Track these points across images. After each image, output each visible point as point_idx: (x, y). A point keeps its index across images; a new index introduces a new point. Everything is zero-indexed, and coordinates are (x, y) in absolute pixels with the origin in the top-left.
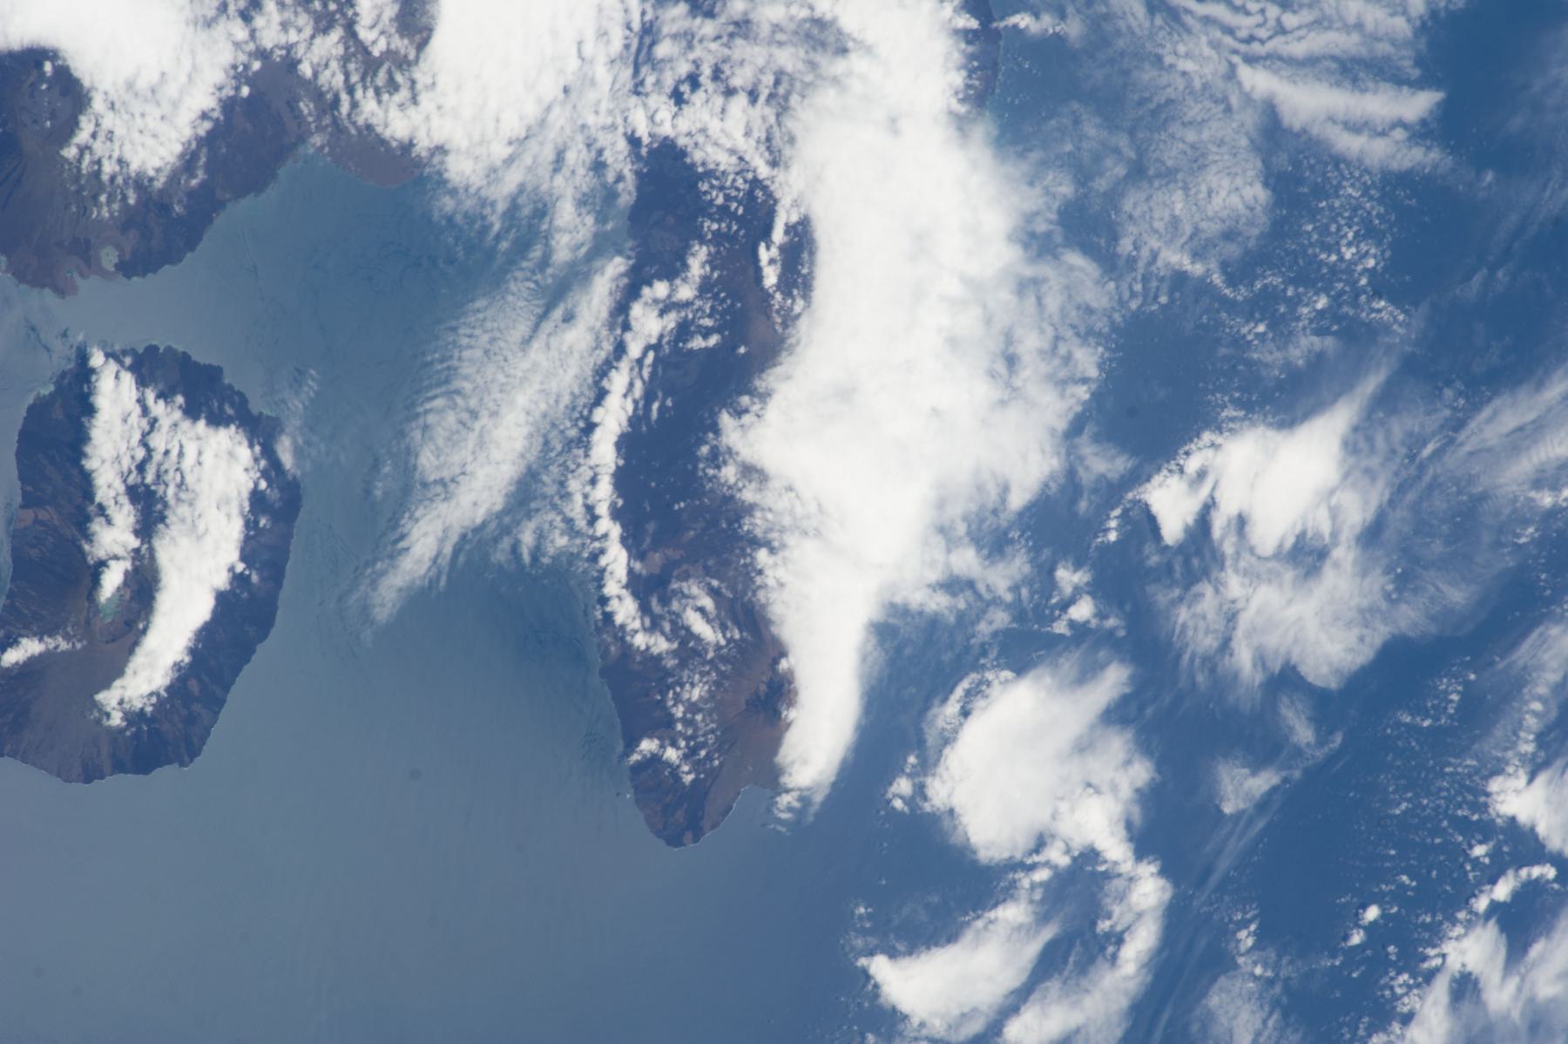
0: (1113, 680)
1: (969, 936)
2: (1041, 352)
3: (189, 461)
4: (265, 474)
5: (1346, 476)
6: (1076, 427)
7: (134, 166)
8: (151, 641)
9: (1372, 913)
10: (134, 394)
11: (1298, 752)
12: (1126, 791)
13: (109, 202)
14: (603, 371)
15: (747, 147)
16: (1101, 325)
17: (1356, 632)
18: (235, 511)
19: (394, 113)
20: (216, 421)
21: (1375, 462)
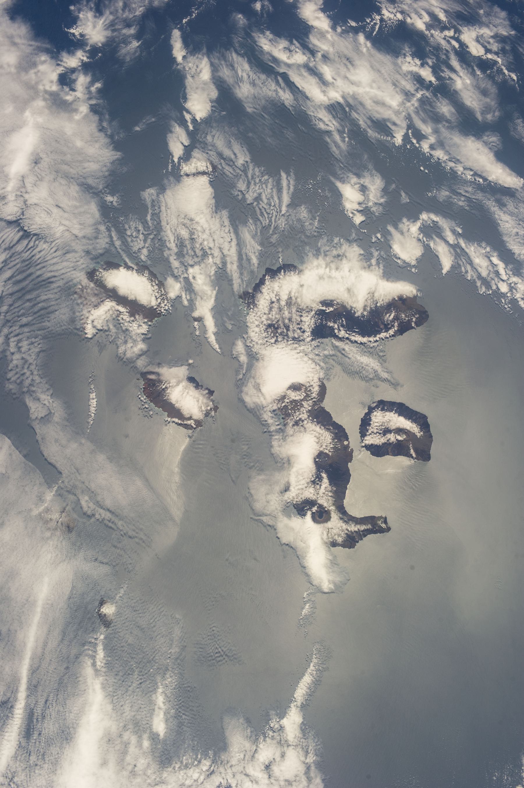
0: (390, 228)
1: (437, 253)
2: (336, 250)
3: (378, 424)
4: (378, 409)
5: (349, 182)
6: (348, 240)
7: (331, 441)
8: (408, 428)
10: (368, 437)
13: (337, 445)
14: (352, 342)
15: (310, 316)
16: (329, 237)
18: (384, 414)
19: (315, 390)
21: (345, 176)
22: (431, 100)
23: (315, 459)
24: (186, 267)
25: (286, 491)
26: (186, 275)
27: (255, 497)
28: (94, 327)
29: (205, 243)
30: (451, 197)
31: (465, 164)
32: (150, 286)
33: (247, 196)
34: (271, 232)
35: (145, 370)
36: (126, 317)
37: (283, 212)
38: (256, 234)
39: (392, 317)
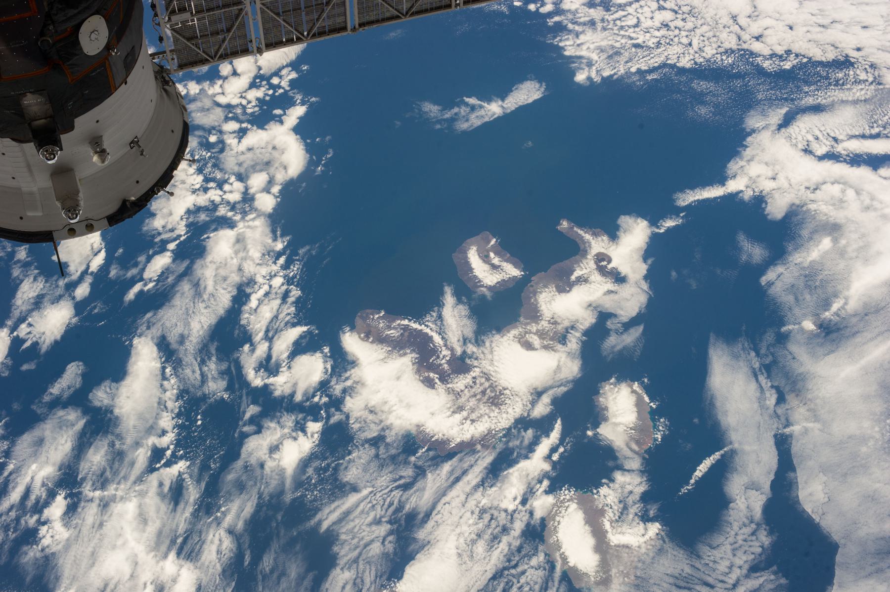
0: (298, 397)
6: (348, 417)
8: (477, 257)
9: (199, 423)
11: (244, 425)
12: (279, 388)
15: (455, 386)
17: (250, 450)
20: (498, 283)
21: (274, 474)
22: (94, 477)
23: (568, 292)
24: (512, 515)
25: (612, 292)
26: (520, 507)
27: (639, 305)
28: (646, 529)
29: (471, 522)
30: (214, 378)
31: (158, 394)
32: (562, 524)
33: (383, 533)
34: (402, 482)
35: (636, 456)
36: (610, 514)
37: (370, 489)
38: (417, 490)
39: (392, 332)
